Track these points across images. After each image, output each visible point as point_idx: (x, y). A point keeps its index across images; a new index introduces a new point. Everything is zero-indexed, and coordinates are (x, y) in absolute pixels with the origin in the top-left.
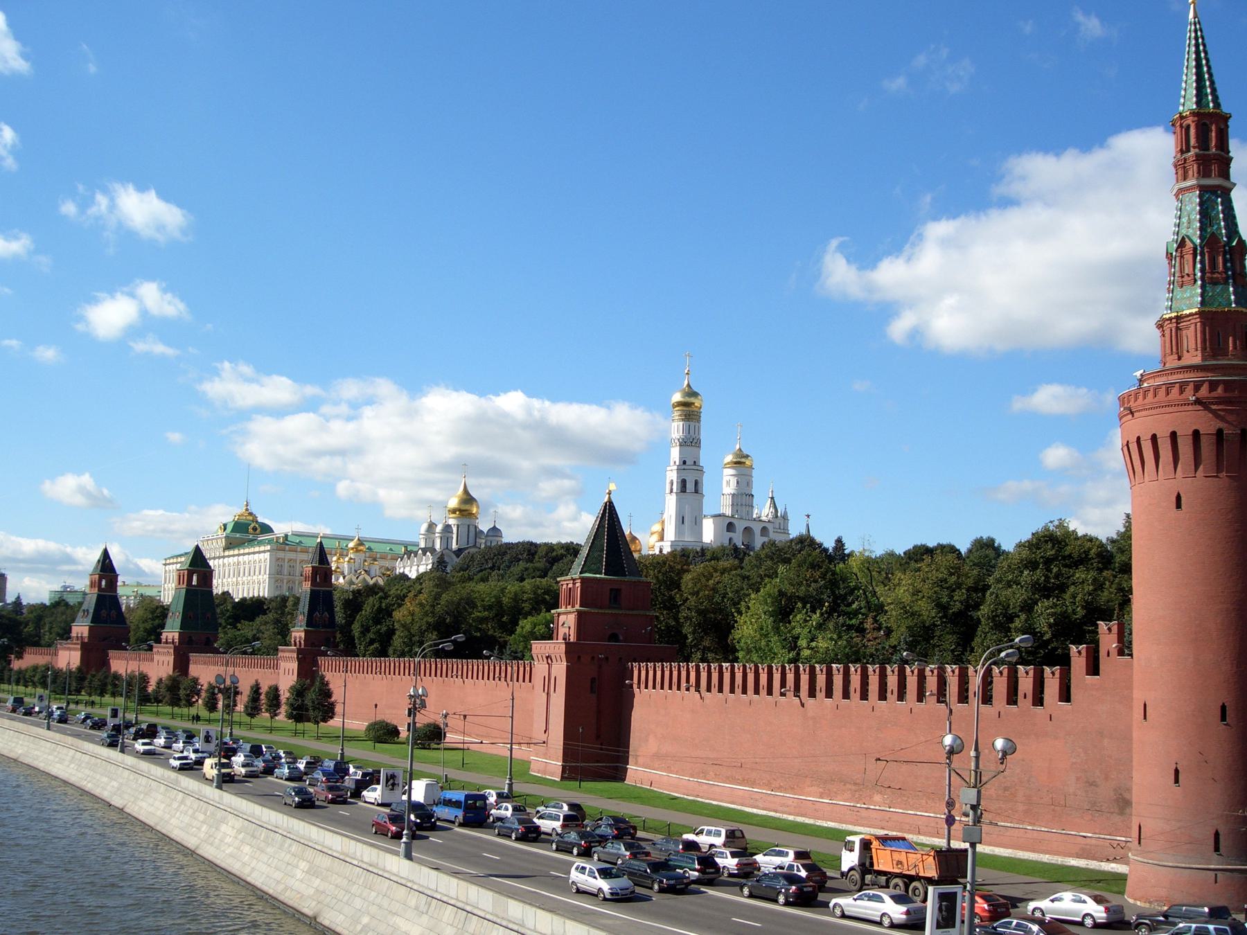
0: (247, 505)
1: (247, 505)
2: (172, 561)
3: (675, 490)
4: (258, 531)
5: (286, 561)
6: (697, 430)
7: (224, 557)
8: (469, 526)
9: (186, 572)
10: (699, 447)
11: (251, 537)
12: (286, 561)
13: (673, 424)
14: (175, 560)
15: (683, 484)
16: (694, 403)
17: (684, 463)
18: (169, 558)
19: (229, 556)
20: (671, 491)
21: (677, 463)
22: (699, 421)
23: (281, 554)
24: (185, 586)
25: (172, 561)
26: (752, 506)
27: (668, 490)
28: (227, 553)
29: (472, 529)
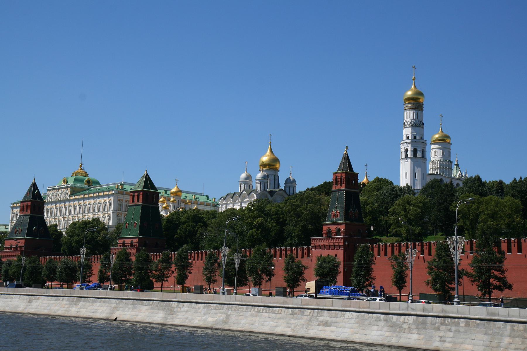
0: (81, 166)
3: (409, 156)
5: (124, 202)
6: (422, 116)
7: (69, 201)
8: (275, 176)
9: (141, 193)
10: (423, 127)
11: (87, 187)
12: (124, 202)
13: (405, 112)
15: (415, 151)
16: (419, 99)
17: (415, 137)
19: (74, 200)
20: (407, 156)
21: (410, 138)
22: (422, 110)
23: (121, 197)
24: (140, 203)
26: (452, 169)
27: (403, 155)
28: (73, 198)
29: (276, 177)
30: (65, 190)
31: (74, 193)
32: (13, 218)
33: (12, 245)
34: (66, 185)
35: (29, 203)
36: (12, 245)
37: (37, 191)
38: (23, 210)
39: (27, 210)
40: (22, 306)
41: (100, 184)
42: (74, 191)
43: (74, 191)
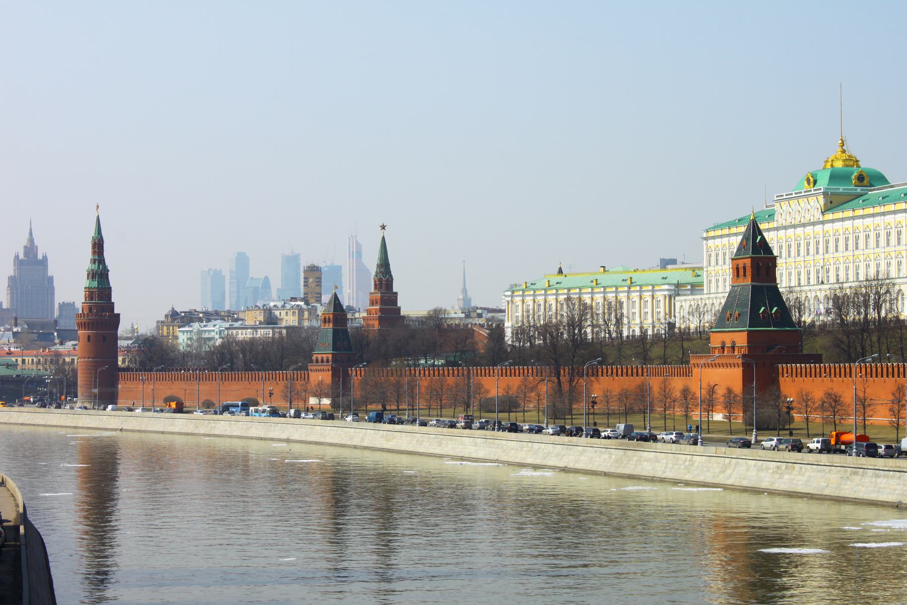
0: (843, 144)
1: (843, 144)
2: (719, 233)
4: (865, 182)
7: (823, 223)
14: (726, 231)
18: (715, 228)
25: (719, 233)
28: (829, 216)
30: (812, 200)
31: (833, 205)
32: (710, 261)
33: (723, 343)
34: (814, 190)
35: (748, 262)
36: (723, 343)
37: (759, 237)
38: (738, 276)
39: (745, 275)
40: (767, 479)
41: (889, 183)
42: (833, 203)
43: (831, 202)
